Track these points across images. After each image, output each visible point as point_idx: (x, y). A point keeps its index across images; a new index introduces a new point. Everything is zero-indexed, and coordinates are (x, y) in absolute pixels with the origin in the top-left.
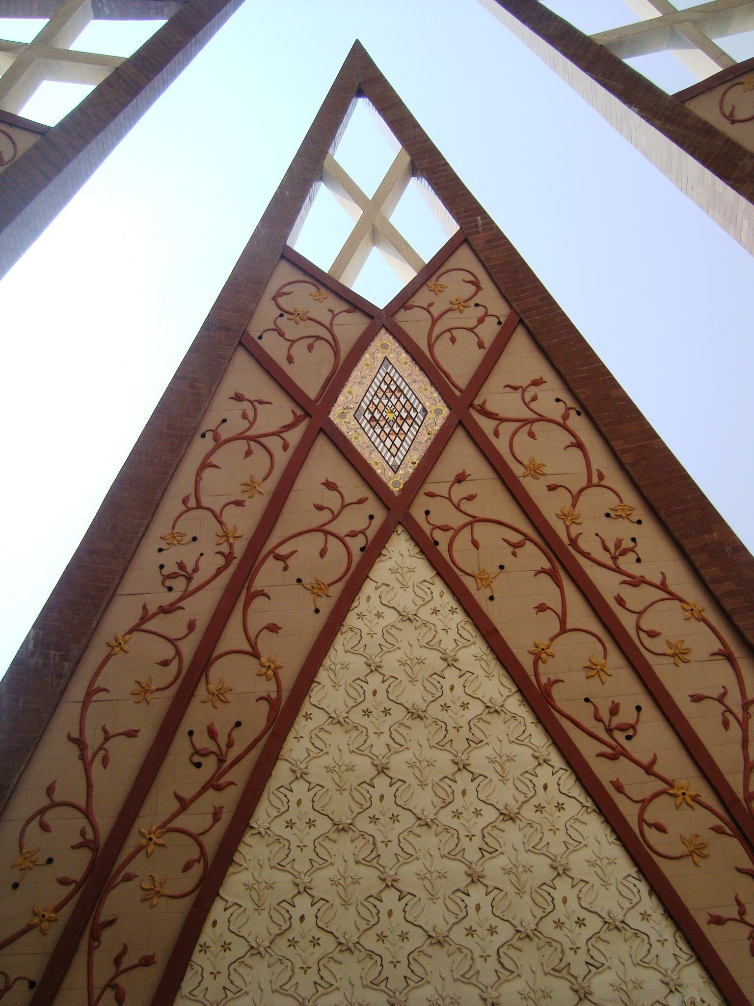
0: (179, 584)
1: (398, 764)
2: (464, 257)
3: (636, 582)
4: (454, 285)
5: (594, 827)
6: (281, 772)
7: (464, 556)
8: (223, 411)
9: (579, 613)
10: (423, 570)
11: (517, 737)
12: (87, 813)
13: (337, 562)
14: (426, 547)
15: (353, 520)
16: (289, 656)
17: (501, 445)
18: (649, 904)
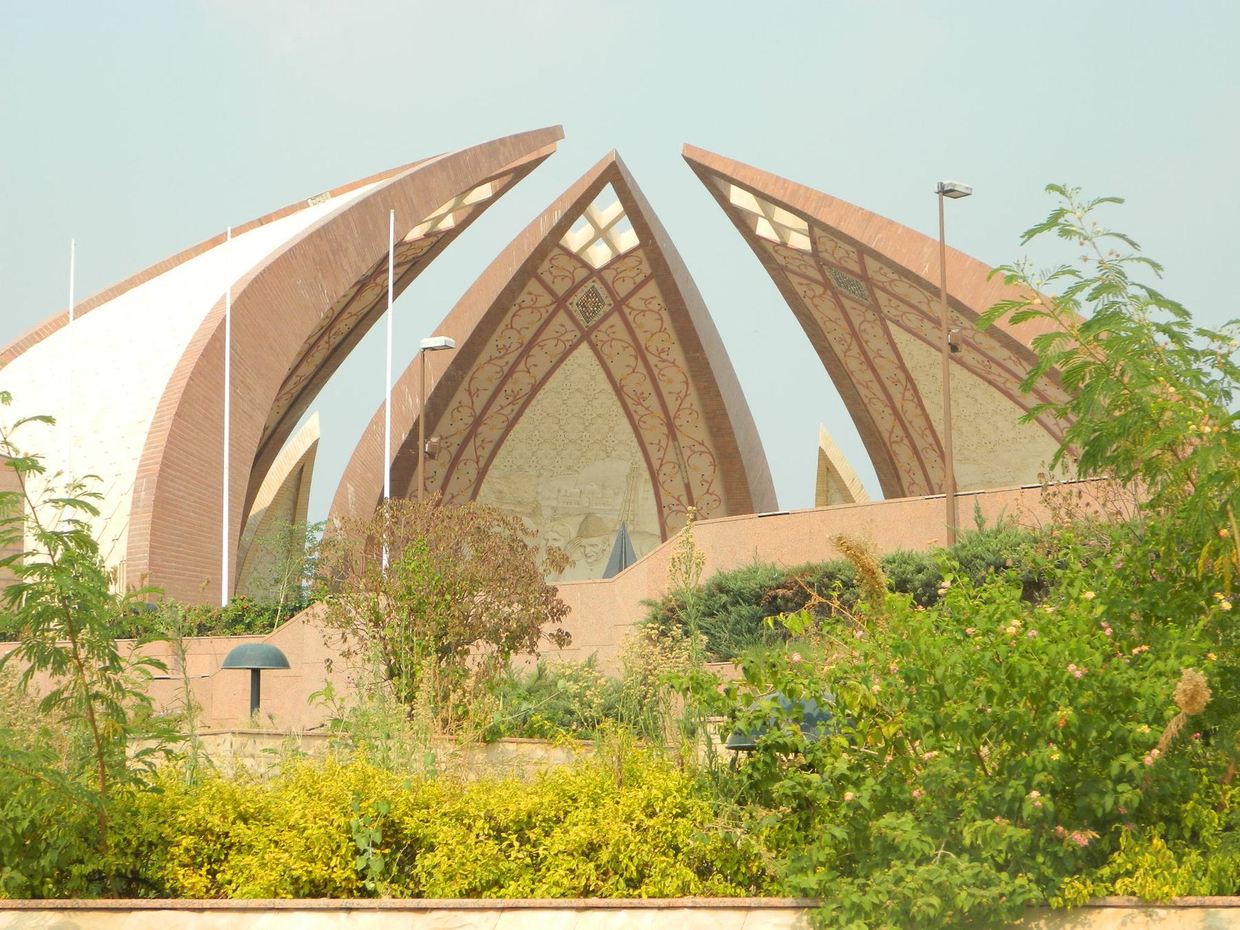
0: (503, 352)
1: (570, 402)
2: (640, 253)
3: (664, 361)
4: (631, 262)
5: (625, 421)
6: (534, 402)
7: (606, 349)
8: (524, 296)
9: (641, 368)
10: (590, 353)
11: (609, 399)
12: (472, 408)
13: (561, 347)
14: (593, 347)
15: (570, 336)
16: (539, 374)
17: (630, 318)
18: (634, 439)
